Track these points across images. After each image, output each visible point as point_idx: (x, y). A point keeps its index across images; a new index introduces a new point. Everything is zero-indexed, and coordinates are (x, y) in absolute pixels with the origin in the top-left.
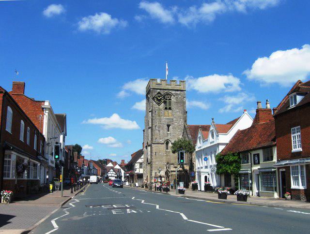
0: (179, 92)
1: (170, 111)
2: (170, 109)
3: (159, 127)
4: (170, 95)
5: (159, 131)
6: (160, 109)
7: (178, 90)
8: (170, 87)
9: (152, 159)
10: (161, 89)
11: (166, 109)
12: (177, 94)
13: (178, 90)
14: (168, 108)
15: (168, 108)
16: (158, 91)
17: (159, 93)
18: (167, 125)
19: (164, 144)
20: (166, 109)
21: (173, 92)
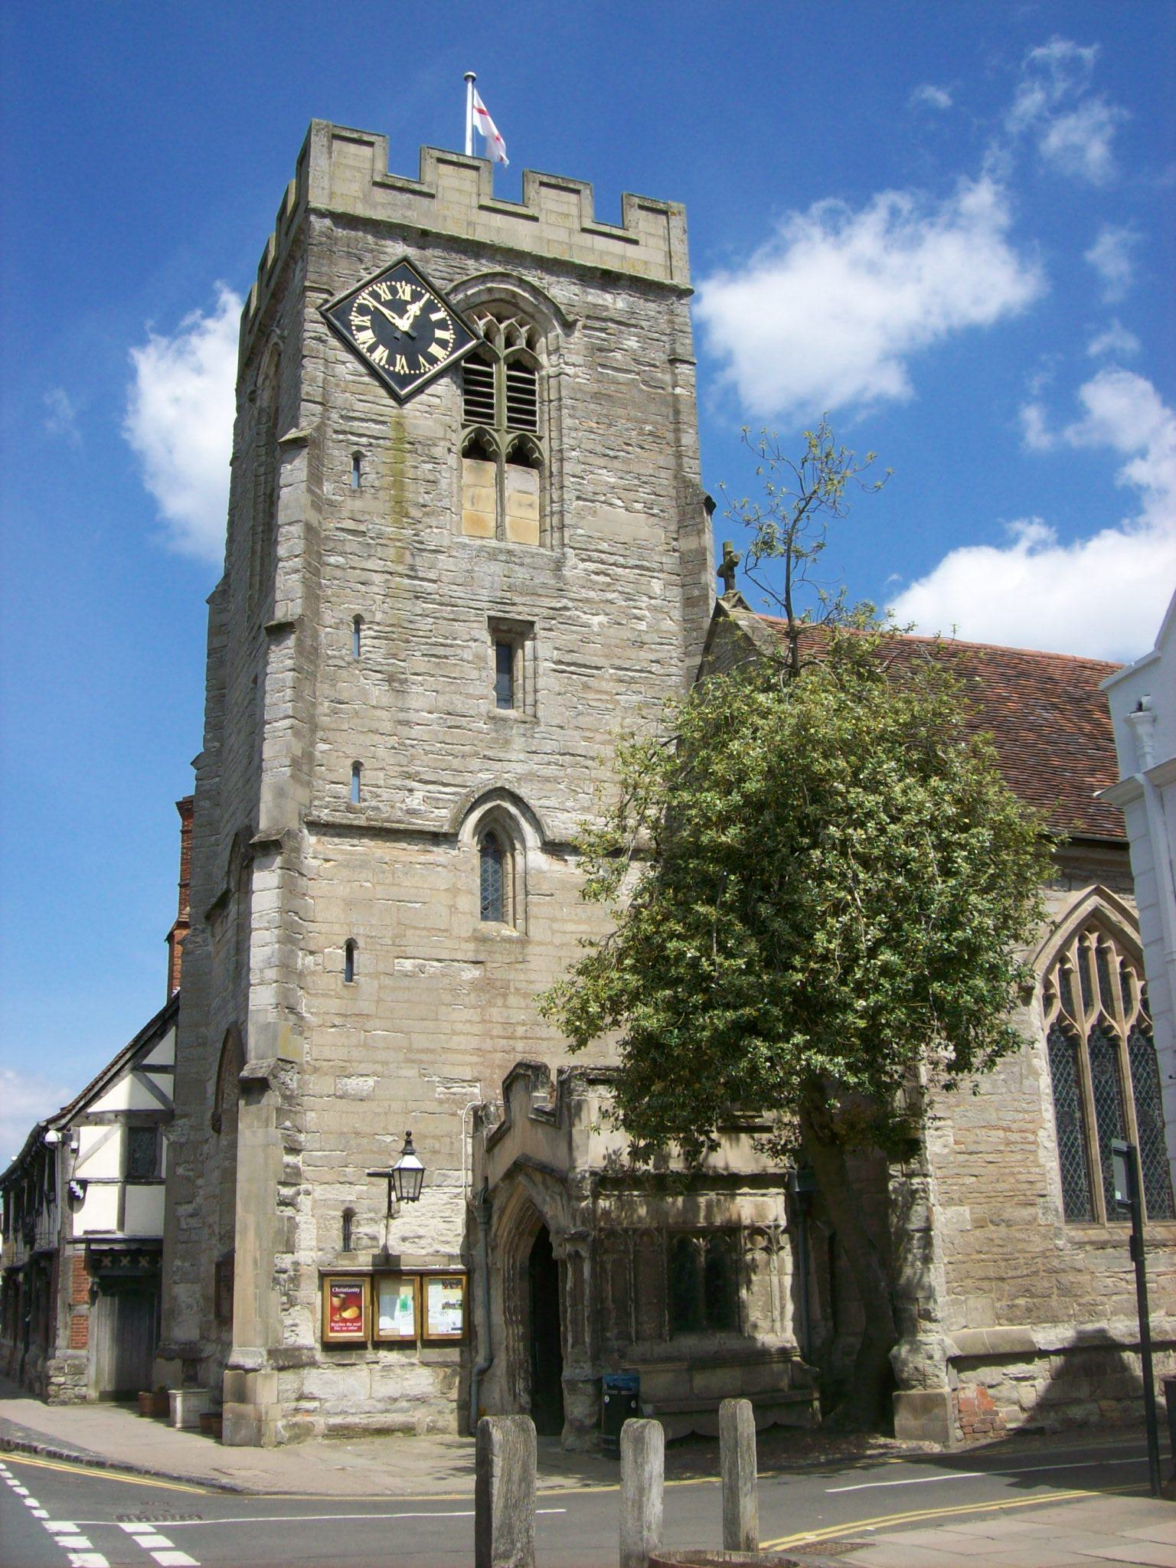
0: (616, 302)
1: (518, 479)
2: (523, 456)
3: (398, 635)
4: (528, 316)
5: (395, 681)
6: (405, 443)
7: (608, 279)
8: (520, 236)
9: (300, 1027)
10: (423, 238)
11: (477, 449)
12: (597, 318)
13: (608, 279)
14: (504, 440)
15: (504, 440)
16: (398, 249)
17: (404, 270)
18: (497, 626)
19: (436, 838)
20: (477, 449)
21: (562, 291)
